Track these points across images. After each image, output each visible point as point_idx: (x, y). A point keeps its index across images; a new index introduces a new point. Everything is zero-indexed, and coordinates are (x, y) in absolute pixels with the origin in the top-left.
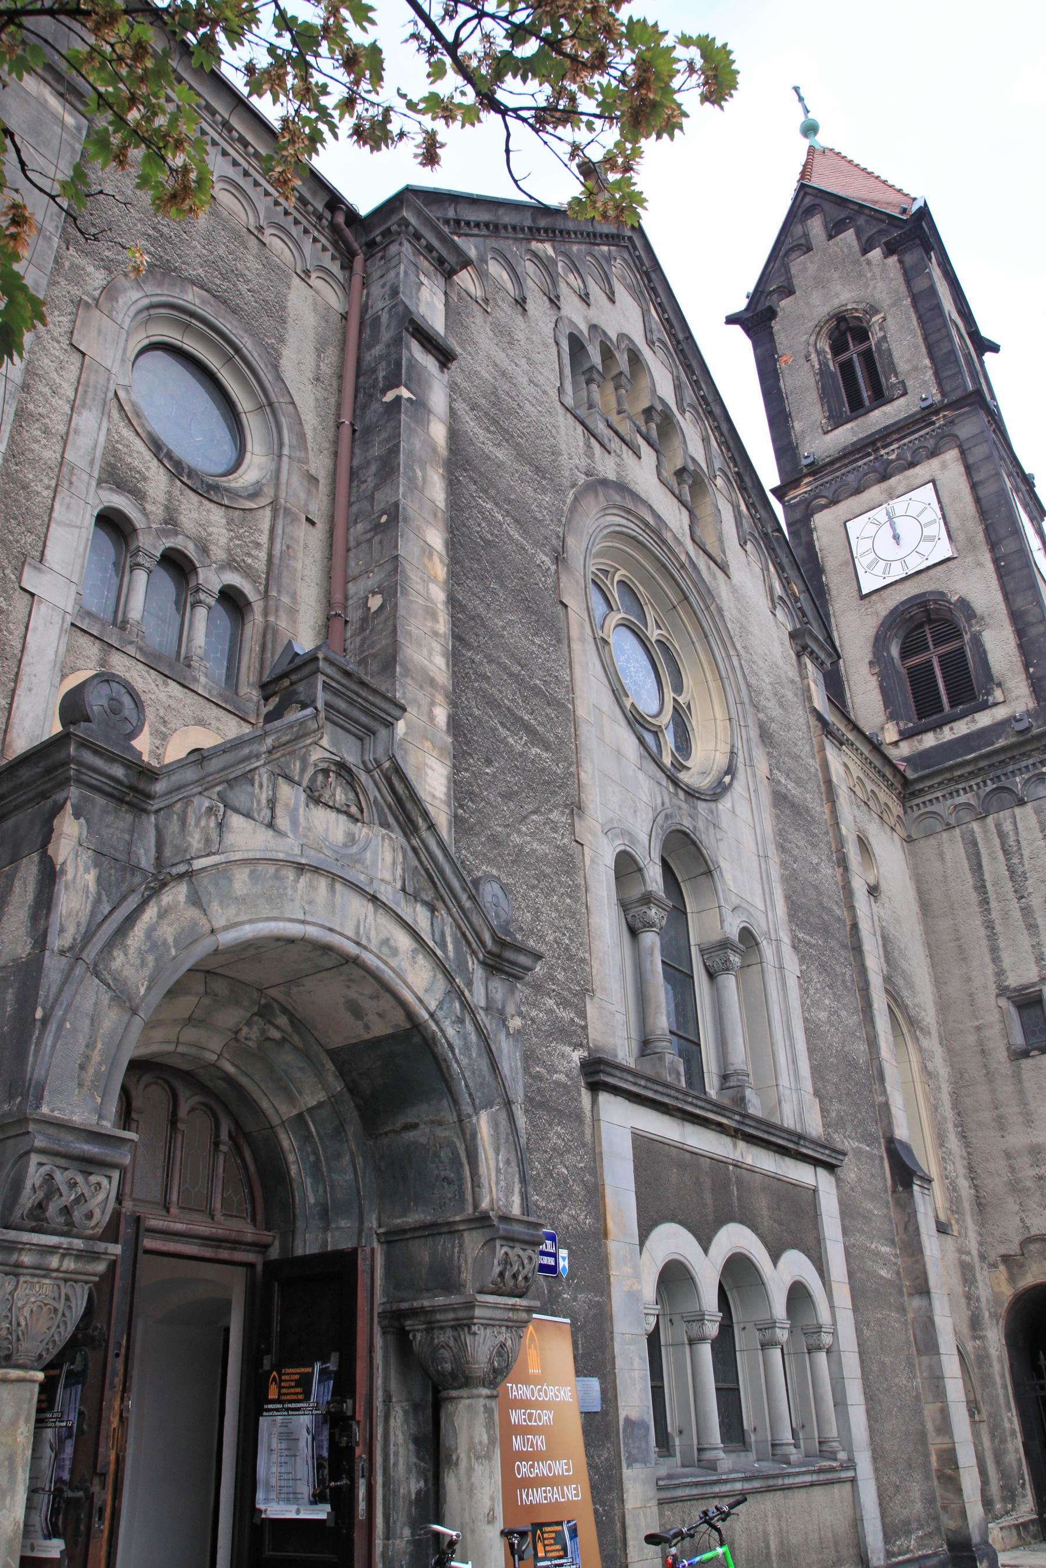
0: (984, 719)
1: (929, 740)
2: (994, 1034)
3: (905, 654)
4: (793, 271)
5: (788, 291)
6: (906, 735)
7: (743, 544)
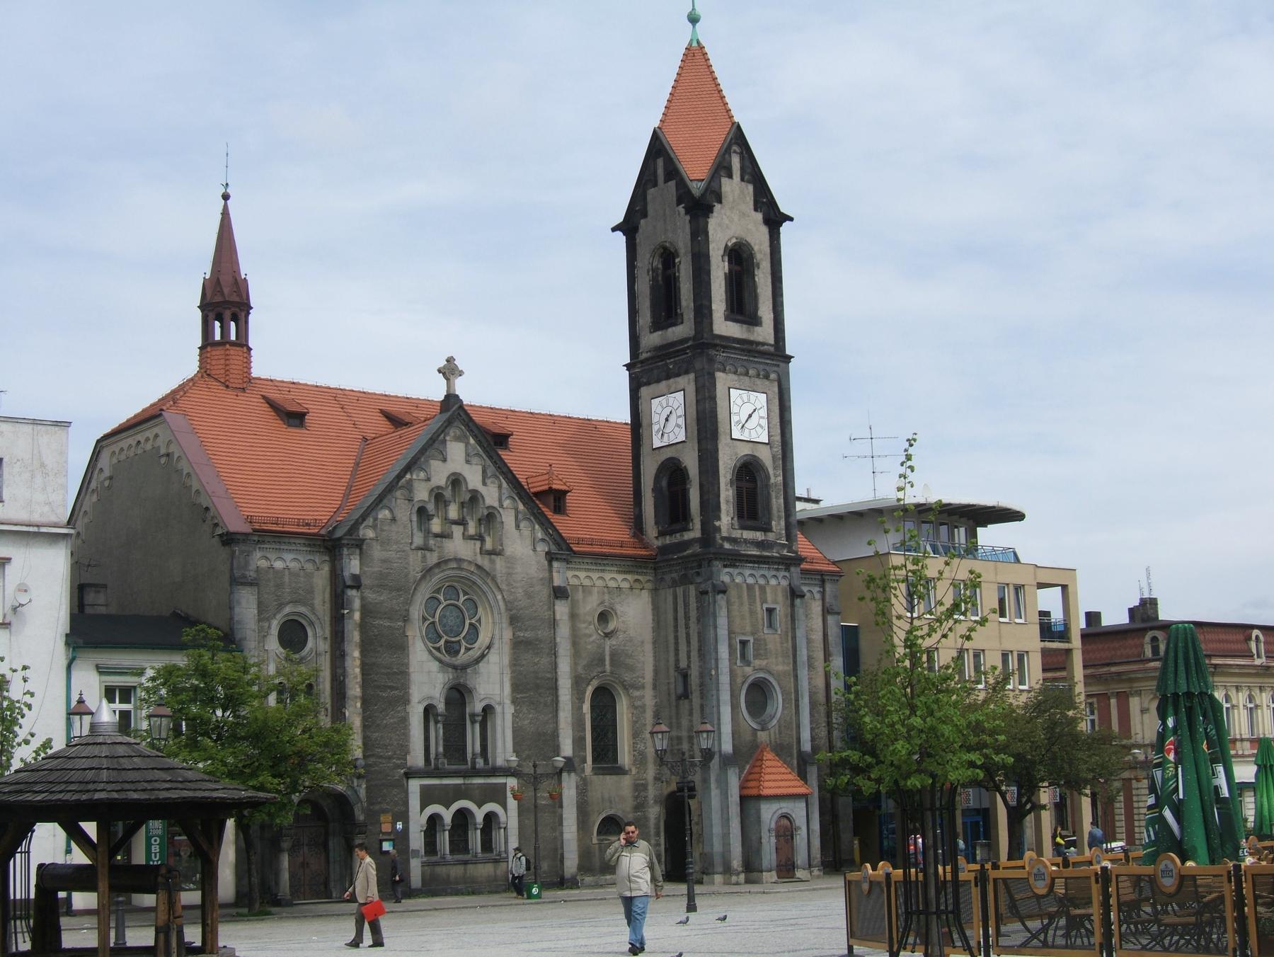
0: (688, 536)
1: (668, 540)
2: (672, 686)
3: (670, 484)
4: (649, 197)
5: (645, 215)
6: (662, 534)
7: (517, 527)
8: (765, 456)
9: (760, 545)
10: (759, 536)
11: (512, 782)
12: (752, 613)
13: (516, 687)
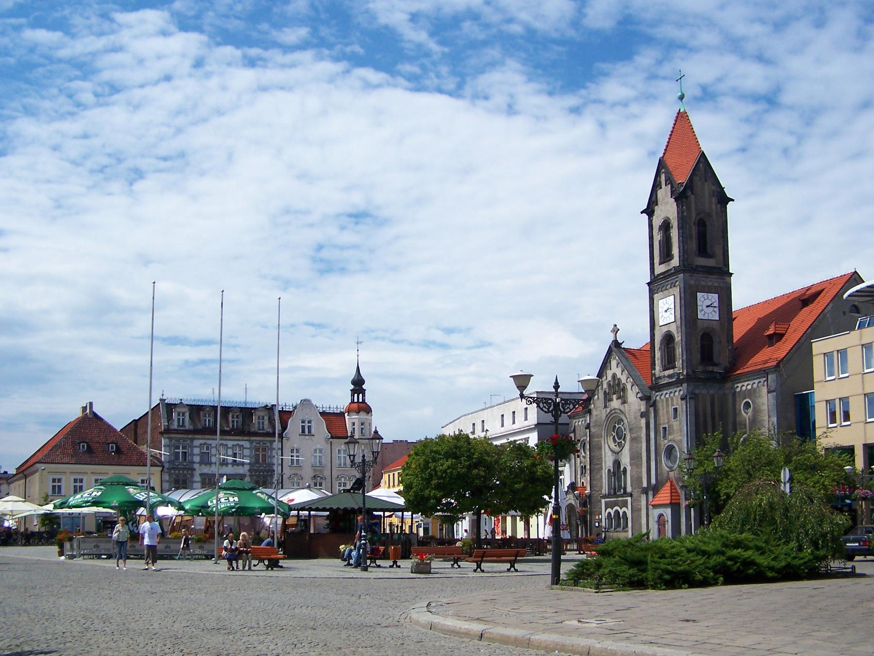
8: (673, 329)
9: (670, 376)
10: (671, 372)
11: (629, 499)
12: (667, 412)
13: (632, 458)
